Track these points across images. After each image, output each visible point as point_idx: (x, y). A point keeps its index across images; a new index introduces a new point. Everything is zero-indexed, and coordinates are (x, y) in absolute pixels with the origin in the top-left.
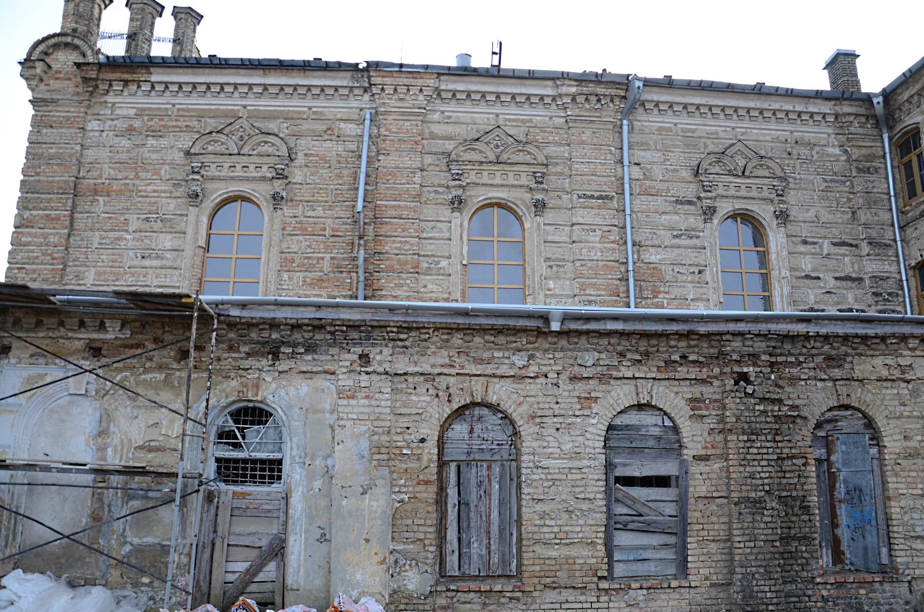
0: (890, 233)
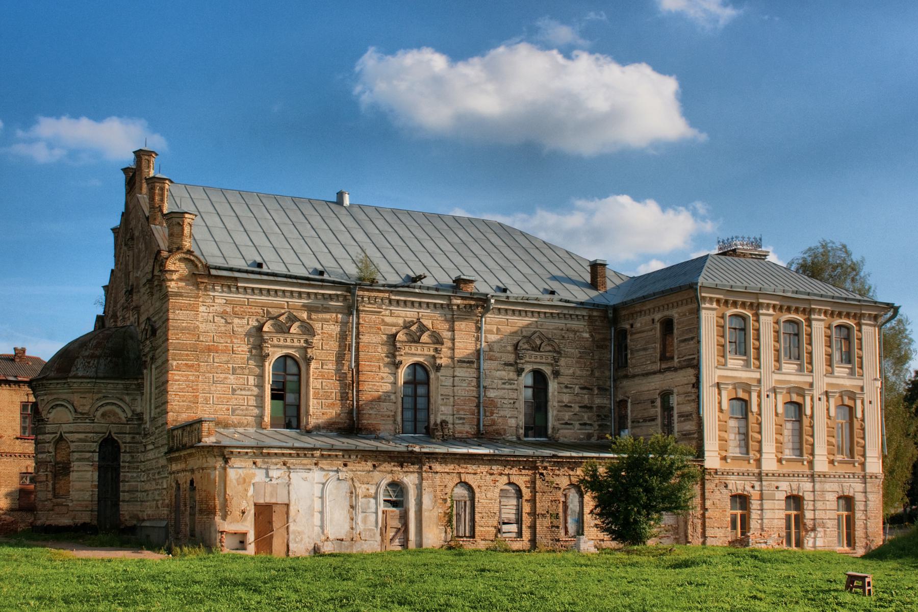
0: (609, 383)
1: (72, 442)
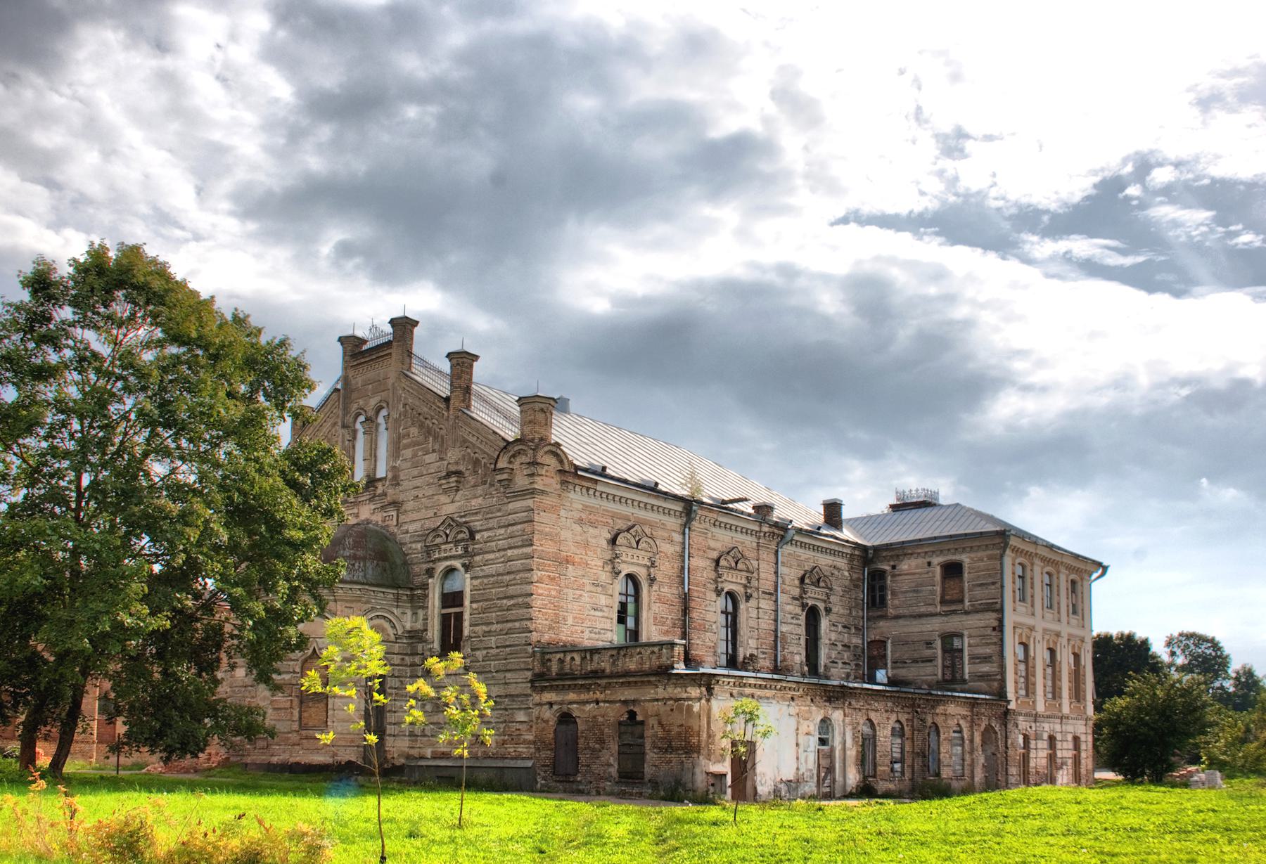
0: (861, 622)
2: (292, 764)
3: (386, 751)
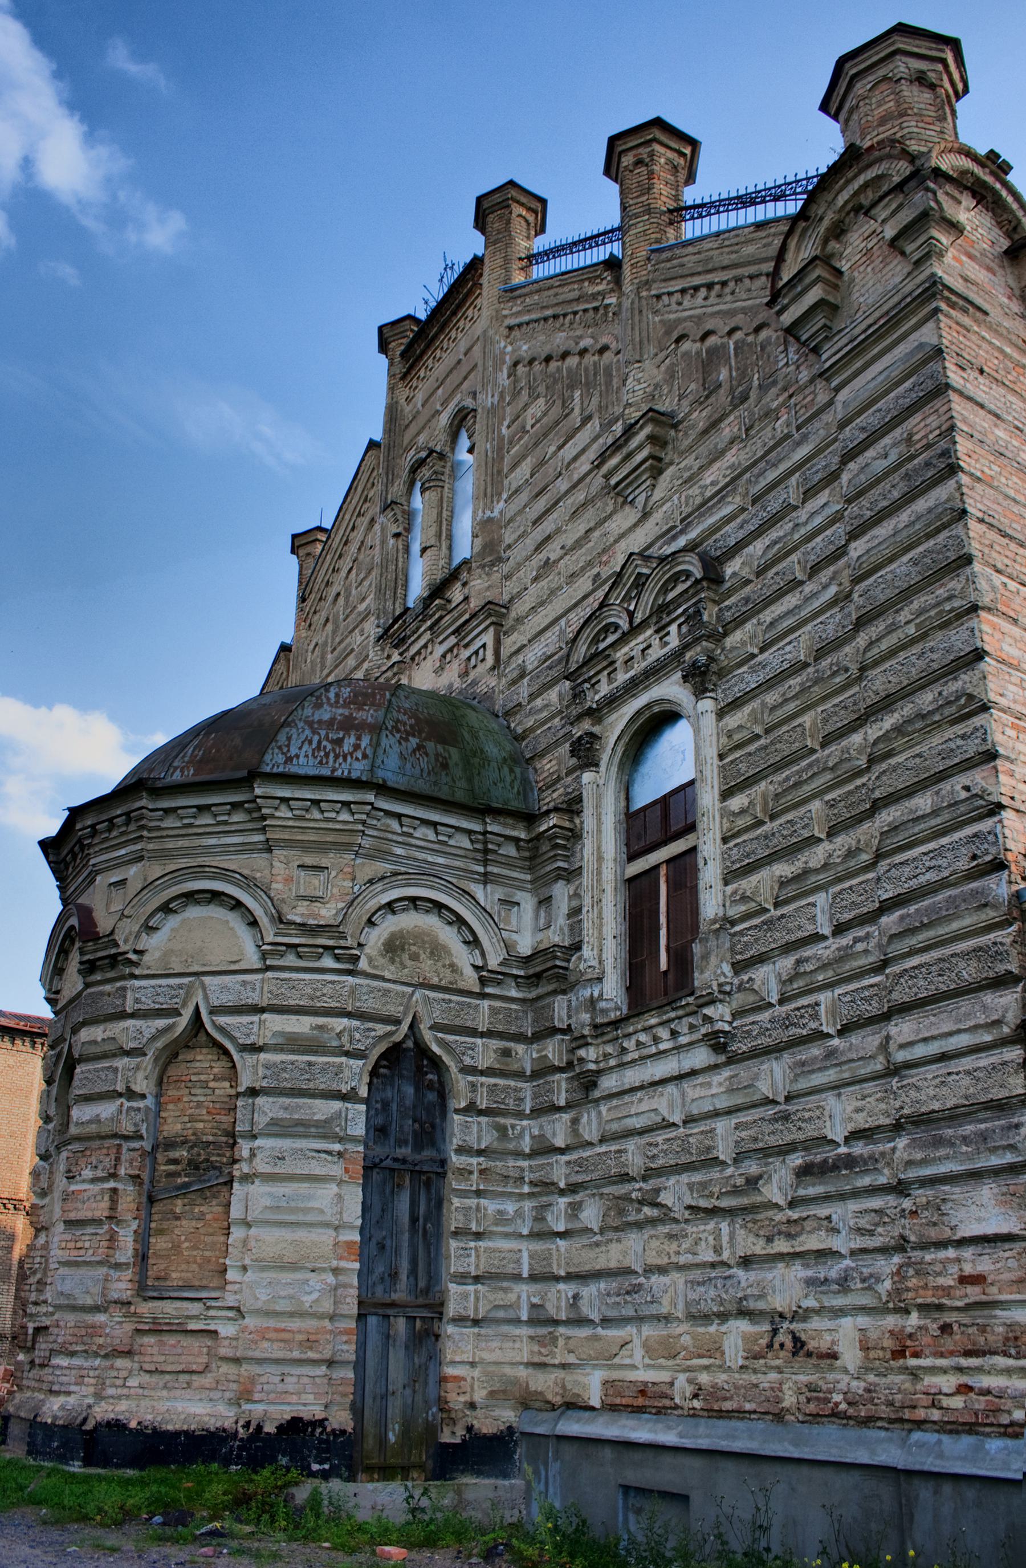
1: (255, 1049)
2: (98, 1425)
3: (443, 1379)
